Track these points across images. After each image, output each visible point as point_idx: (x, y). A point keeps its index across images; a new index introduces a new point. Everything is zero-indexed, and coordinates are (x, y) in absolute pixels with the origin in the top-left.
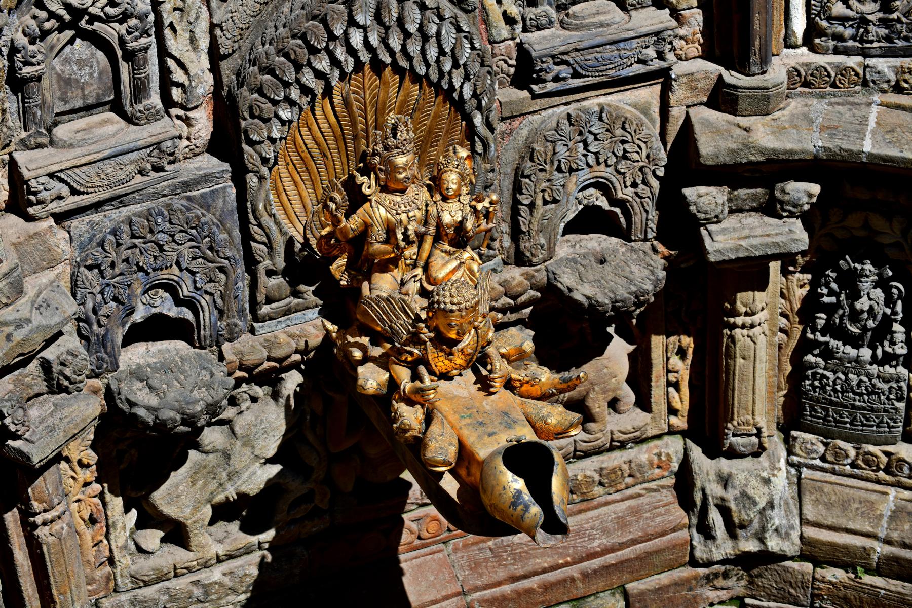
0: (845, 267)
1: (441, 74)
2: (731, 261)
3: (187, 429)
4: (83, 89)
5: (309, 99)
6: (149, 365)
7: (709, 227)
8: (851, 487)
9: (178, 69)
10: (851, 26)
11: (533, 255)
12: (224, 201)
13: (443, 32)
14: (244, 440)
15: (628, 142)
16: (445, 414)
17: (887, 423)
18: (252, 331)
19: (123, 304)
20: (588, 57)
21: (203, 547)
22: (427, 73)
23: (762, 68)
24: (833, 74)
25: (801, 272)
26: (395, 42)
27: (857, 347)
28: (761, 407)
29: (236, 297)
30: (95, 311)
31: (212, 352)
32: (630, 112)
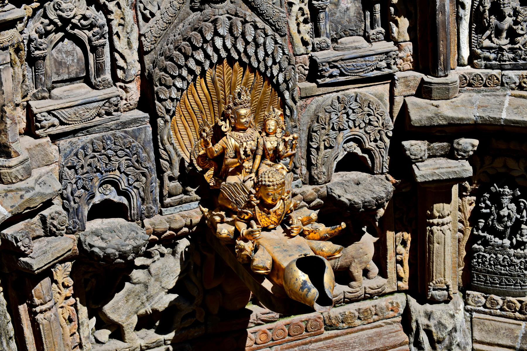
0: (494, 191)
1: (266, 67)
2: (429, 181)
3: (122, 261)
4: (68, 68)
6: (102, 229)
7: (417, 164)
8: (500, 322)
9: (121, 59)
10: (494, 52)
12: (145, 135)
13: (267, 43)
14: (156, 277)
15: (372, 115)
16: (265, 246)
17: (520, 283)
18: (161, 213)
19: (88, 191)
20: (348, 64)
21: (132, 340)
22: (258, 66)
23: (445, 73)
24: (485, 79)
25: (470, 196)
26: (240, 46)
27: (502, 238)
28: (448, 273)
29: (152, 192)
30: (72, 194)
31: (138, 224)
32: (373, 99)
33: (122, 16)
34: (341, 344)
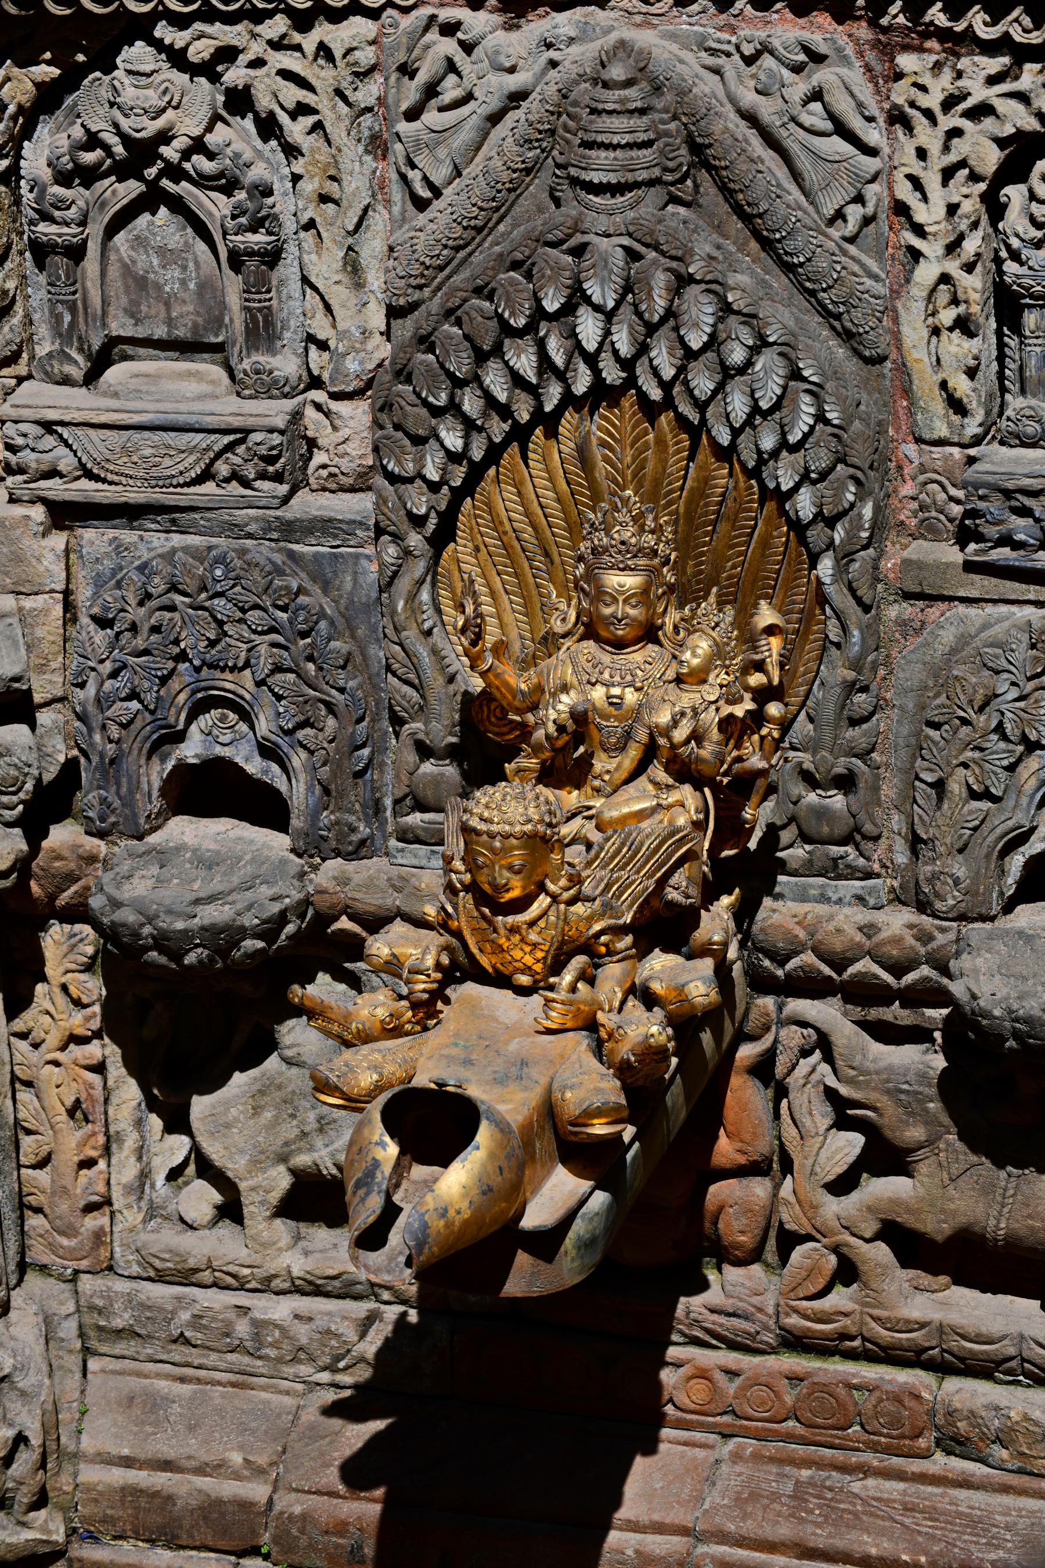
3: (163, 960)
4: (168, 305)
5: (506, 427)
11: (937, 895)
12: (355, 580)
22: (733, 444)
29: (359, 774)
33: (332, 172)
34: (960, 1515)
